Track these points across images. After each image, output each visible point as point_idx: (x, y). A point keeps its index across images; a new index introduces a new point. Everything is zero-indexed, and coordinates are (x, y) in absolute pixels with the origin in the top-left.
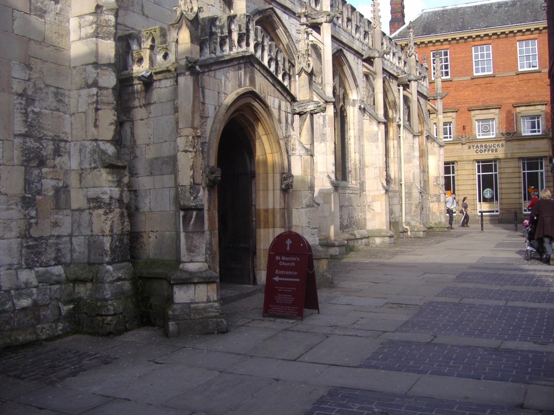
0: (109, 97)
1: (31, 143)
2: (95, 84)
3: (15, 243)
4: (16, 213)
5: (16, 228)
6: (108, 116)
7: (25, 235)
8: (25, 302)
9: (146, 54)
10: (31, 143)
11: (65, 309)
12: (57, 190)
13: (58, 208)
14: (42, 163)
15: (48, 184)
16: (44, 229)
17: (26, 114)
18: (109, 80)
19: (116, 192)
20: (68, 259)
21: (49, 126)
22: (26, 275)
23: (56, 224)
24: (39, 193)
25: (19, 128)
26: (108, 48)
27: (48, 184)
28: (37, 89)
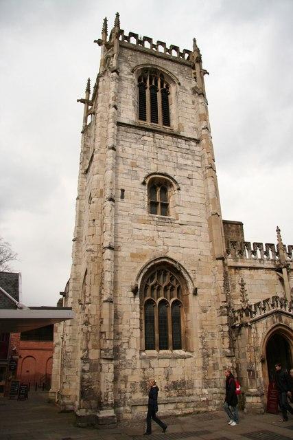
0: (227, 334)
1: (204, 351)
2: (222, 331)
3: (201, 381)
4: (201, 372)
5: (201, 376)
6: (227, 340)
7: (204, 378)
8: (204, 399)
9: (239, 317)
10: (204, 351)
11: (218, 402)
12: (214, 364)
13: (214, 369)
14: (208, 356)
15: (211, 363)
16: (210, 376)
17: (202, 342)
18: (226, 329)
19: (231, 365)
20: (219, 386)
21: (210, 345)
22: (205, 391)
23: (214, 375)
24: (208, 365)
25: (201, 347)
26: (225, 319)
27: (211, 363)
28: (205, 334)
